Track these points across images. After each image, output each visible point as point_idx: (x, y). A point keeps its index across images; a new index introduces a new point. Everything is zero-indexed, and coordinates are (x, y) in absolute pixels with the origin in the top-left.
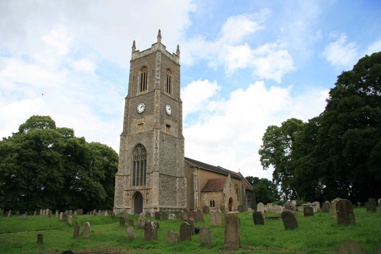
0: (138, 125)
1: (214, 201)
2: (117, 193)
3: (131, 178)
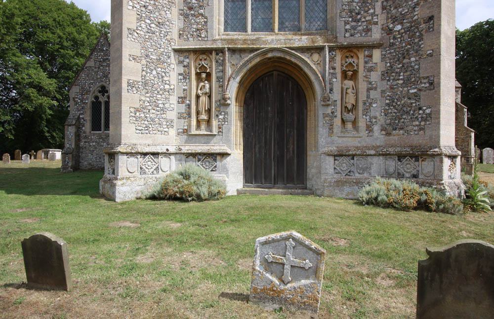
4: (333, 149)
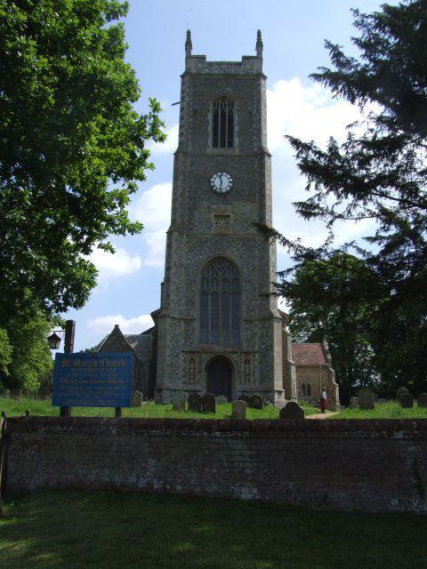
0: (216, 216)
1: (309, 386)
2: (169, 356)
3: (196, 324)
4: (241, 390)
